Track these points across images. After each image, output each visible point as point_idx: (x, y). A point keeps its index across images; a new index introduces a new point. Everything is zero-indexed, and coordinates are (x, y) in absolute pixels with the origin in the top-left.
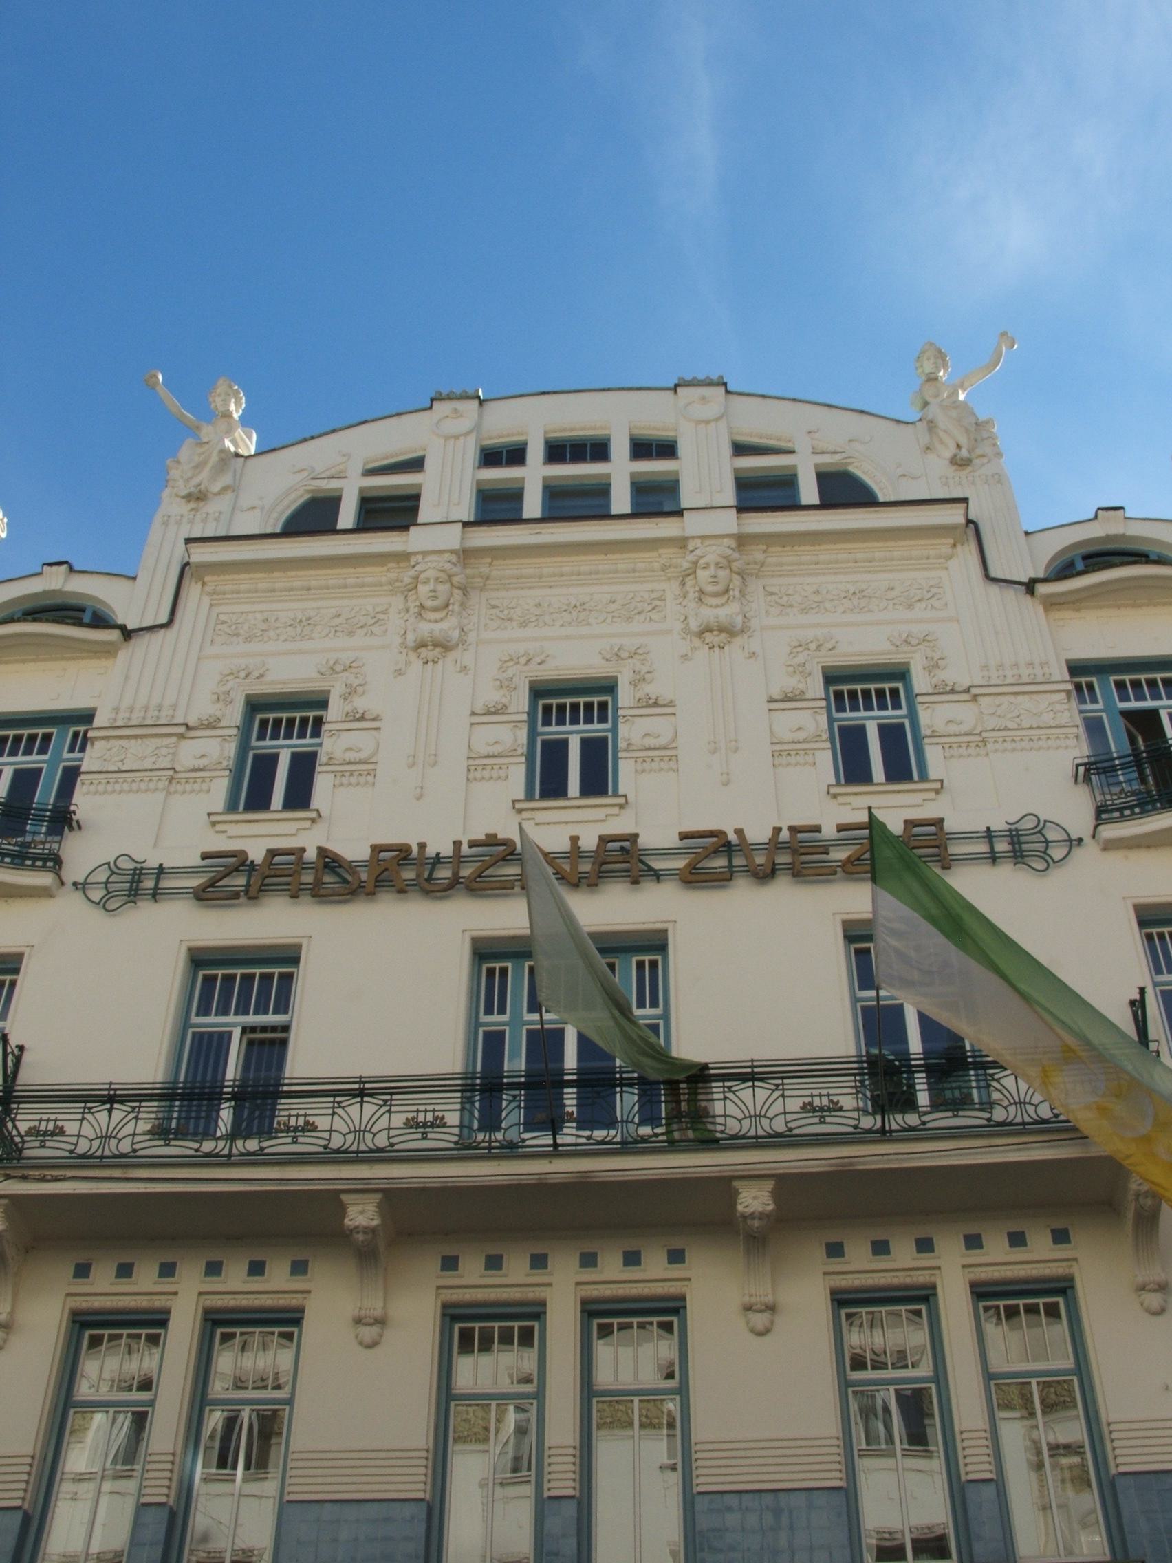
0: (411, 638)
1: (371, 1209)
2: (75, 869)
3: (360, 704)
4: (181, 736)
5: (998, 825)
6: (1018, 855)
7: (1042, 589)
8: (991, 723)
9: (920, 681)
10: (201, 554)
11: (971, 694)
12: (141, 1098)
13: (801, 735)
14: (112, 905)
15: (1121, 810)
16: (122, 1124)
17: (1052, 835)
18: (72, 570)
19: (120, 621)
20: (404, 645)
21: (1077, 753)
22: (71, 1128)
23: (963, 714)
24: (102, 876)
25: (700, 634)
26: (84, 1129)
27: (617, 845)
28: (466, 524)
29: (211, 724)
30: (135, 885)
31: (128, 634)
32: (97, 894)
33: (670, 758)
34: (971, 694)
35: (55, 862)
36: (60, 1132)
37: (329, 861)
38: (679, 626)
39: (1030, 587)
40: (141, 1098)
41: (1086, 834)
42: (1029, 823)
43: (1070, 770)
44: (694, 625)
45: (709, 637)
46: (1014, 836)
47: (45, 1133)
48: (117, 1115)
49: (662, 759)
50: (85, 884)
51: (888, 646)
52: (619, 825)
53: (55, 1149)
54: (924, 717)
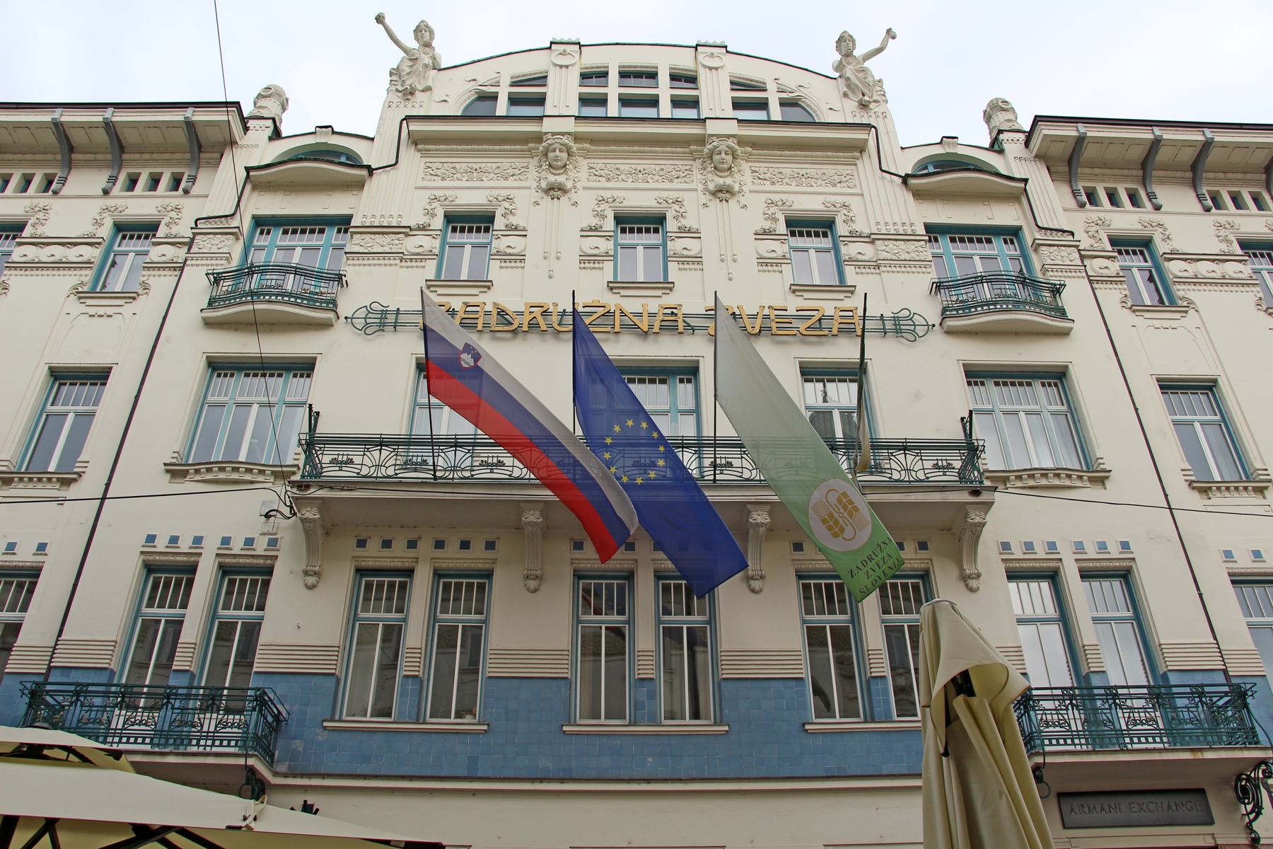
0: (544, 185)
1: (537, 513)
2: (345, 308)
3: (514, 220)
4: (407, 235)
5: (887, 314)
6: (898, 331)
7: (912, 181)
8: (884, 255)
9: (841, 229)
10: (416, 127)
11: (871, 239)
12: (398, 443)
13: (774, 255)
14: (369, 331)
15: (957, 310)
16: (387, 459)
17: (917, 319)
18: (334, 132)
19: (365, 163)
20: (539, 187)
21: (931, 276)
22: (357, 460)
23: (868, 251)
24: (362, 313)
25: (714, 194)
26: (366, 463)
27: (669, 311)
28: (577, 118)
29: (423, 228)
30: (382, 321)
31: (371, 170)
32: (360, 323)
33: (698, 263)
34: (871, 239)
35: (332, 304)
36: (352, 462)
37: (502, 313)
38: (701, 187)
39: (905, 179)
40: (398, 443)
41: (937, 321)
42: (906, 313)
43: (927, 286)
44: (711, 187)
45: (720, 195)
46: (896, 319)
47: (342, 462)
48: (385, 453)
49: (693, 263)
50: (352, 318)
51: (822, 207)
52: (669, 300)
53: (347, 473)
54: (843, 250)
